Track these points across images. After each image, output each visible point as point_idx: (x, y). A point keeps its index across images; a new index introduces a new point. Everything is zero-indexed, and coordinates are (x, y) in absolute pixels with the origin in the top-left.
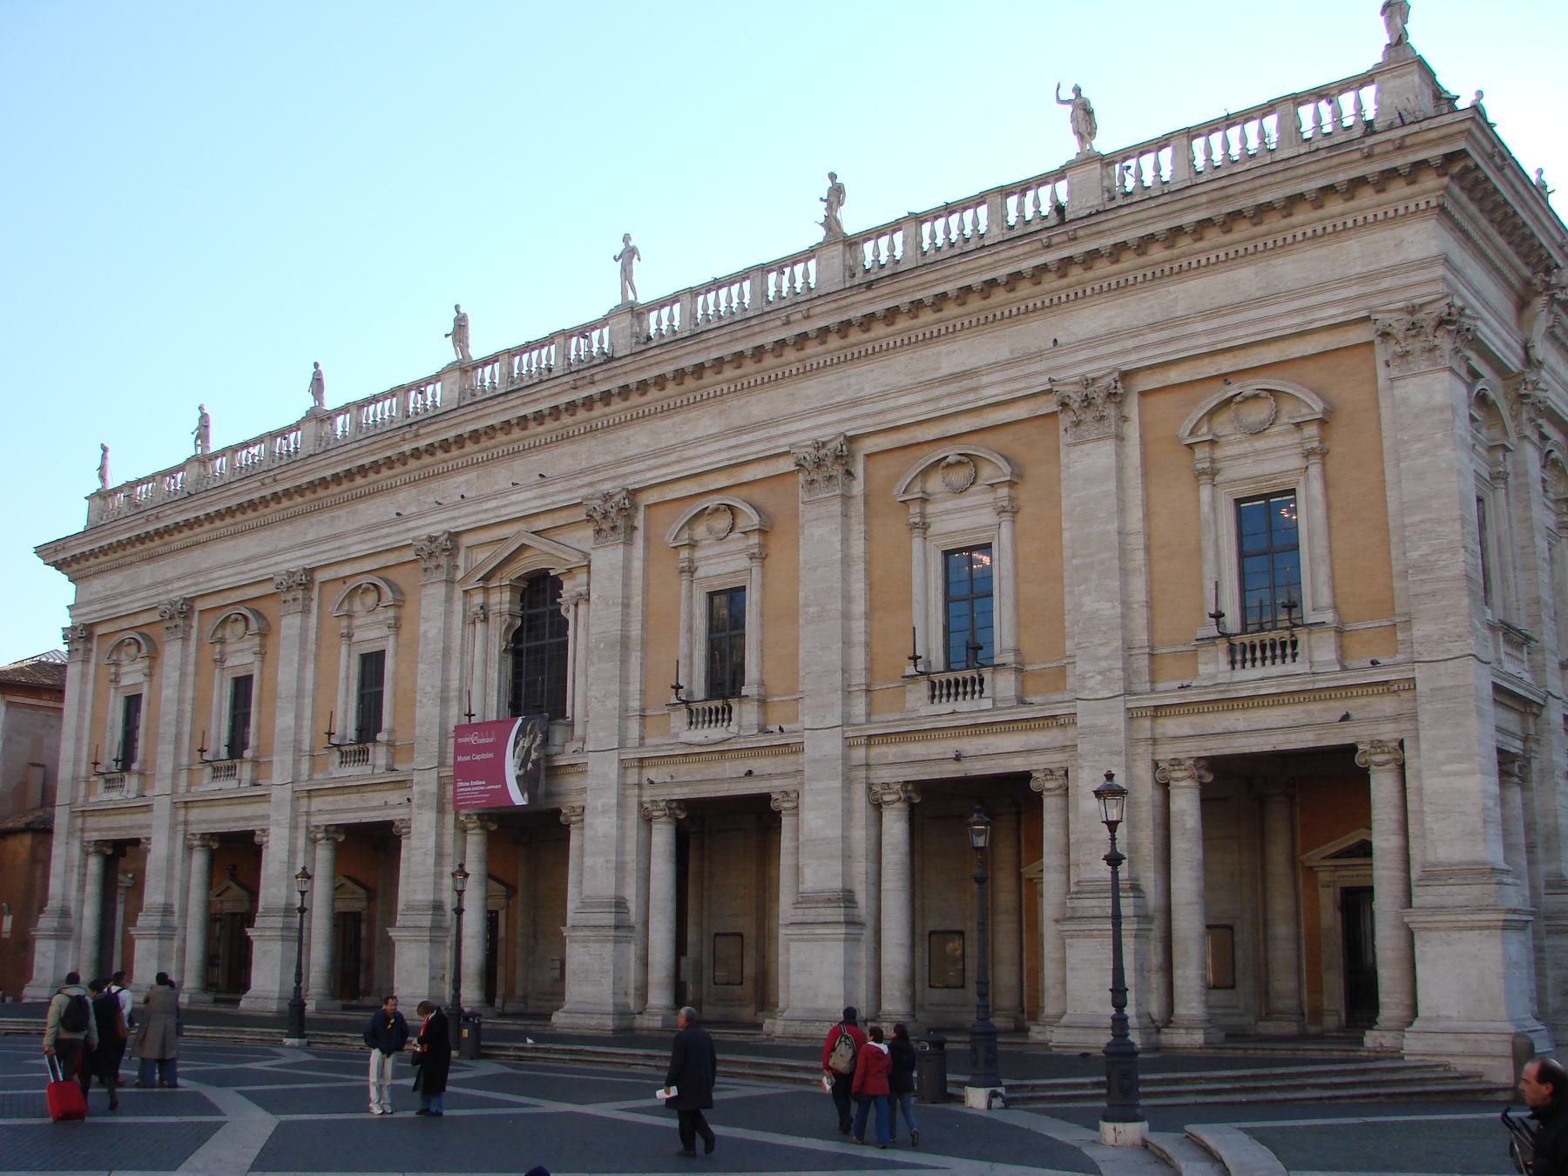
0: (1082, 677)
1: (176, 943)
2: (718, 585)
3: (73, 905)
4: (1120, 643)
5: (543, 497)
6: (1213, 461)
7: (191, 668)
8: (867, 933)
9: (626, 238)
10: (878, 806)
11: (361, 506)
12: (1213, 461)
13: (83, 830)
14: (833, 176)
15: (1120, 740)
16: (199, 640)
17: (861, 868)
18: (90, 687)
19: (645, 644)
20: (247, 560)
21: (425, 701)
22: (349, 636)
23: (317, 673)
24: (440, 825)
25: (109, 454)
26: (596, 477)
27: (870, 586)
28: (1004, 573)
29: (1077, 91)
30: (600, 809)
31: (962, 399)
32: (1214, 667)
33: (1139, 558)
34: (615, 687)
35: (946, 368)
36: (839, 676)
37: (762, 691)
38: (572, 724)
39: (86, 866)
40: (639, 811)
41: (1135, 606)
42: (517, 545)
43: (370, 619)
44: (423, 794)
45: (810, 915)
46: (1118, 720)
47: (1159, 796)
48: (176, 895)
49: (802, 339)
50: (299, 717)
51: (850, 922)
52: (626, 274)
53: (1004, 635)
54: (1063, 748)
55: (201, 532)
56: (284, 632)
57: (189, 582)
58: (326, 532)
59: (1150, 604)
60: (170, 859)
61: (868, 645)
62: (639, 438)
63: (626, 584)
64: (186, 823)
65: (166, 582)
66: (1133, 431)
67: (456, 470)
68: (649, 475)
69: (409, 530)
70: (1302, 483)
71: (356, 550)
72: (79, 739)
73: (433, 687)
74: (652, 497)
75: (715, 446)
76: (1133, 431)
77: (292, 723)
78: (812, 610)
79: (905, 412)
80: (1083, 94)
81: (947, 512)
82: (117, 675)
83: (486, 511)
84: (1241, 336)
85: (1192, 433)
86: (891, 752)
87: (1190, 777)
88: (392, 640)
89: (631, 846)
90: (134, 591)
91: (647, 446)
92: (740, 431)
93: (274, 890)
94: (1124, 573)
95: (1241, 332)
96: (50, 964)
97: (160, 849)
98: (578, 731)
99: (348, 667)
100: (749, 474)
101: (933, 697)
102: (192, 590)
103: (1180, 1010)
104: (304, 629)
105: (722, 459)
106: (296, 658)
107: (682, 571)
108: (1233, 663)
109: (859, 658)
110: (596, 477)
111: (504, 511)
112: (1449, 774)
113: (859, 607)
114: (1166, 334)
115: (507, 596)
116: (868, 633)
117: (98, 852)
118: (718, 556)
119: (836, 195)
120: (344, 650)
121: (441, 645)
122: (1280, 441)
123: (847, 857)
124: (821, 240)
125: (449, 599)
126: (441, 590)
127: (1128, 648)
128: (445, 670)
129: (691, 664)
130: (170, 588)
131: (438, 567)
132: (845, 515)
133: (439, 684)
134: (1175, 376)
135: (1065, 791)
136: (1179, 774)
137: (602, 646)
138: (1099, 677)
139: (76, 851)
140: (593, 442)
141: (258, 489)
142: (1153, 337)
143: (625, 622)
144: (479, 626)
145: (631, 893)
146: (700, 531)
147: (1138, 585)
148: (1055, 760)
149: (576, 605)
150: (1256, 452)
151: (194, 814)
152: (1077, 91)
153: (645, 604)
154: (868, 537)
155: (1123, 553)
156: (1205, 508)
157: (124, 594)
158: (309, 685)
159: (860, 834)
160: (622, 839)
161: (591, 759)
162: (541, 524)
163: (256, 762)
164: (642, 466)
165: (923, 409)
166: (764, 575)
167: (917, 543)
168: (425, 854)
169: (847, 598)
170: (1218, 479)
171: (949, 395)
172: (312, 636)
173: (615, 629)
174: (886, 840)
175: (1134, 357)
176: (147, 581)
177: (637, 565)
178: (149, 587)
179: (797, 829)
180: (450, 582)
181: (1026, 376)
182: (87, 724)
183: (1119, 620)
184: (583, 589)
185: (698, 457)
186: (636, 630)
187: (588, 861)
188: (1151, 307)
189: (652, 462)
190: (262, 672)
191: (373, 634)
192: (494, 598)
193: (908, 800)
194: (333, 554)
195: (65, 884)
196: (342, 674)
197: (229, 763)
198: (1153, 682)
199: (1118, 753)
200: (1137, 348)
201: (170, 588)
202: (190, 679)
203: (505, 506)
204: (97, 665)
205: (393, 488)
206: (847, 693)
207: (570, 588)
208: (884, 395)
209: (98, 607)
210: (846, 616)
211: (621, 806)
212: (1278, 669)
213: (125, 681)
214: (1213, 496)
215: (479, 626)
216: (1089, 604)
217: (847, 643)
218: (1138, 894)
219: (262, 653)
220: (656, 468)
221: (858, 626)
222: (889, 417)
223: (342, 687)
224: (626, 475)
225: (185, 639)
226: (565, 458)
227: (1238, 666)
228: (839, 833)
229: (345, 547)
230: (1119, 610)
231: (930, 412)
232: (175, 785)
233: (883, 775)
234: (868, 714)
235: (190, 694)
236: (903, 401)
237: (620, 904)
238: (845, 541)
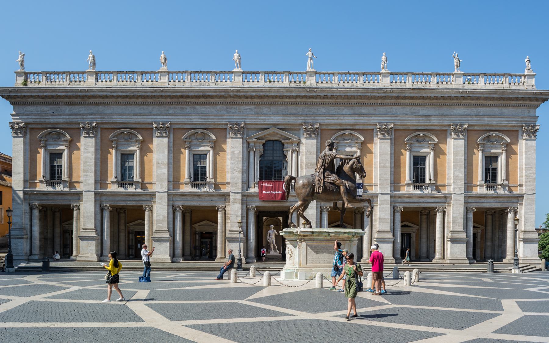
5: (284, 119)
26: (307, 118)
102: (100, 120)
110: (307, 118)
111: (267, 121)
112: (530, 214)
130: (85, 117)
162: (280, 127)
201: (85, 117)
220: (329, 119)
229: (191, 119)
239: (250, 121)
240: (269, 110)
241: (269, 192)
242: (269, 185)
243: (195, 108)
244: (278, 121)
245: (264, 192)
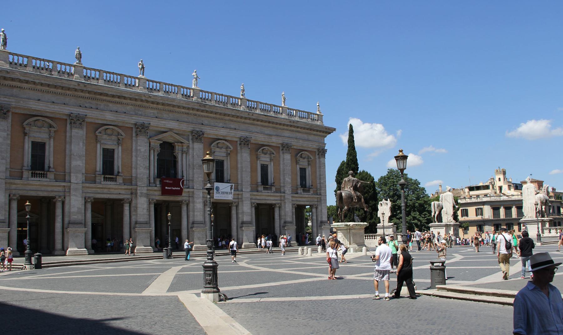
30: (198, 202)
35: (266, 132)
44: (141, 193)
73: (144, 165)
78: (244, 169)
137: (197, 166)
168: (143, 209)
207: (178, 147)
222: (257, 138)
239: (154, 123)
241: (170, 188)
242: (170, 182)
245: (166, 188)
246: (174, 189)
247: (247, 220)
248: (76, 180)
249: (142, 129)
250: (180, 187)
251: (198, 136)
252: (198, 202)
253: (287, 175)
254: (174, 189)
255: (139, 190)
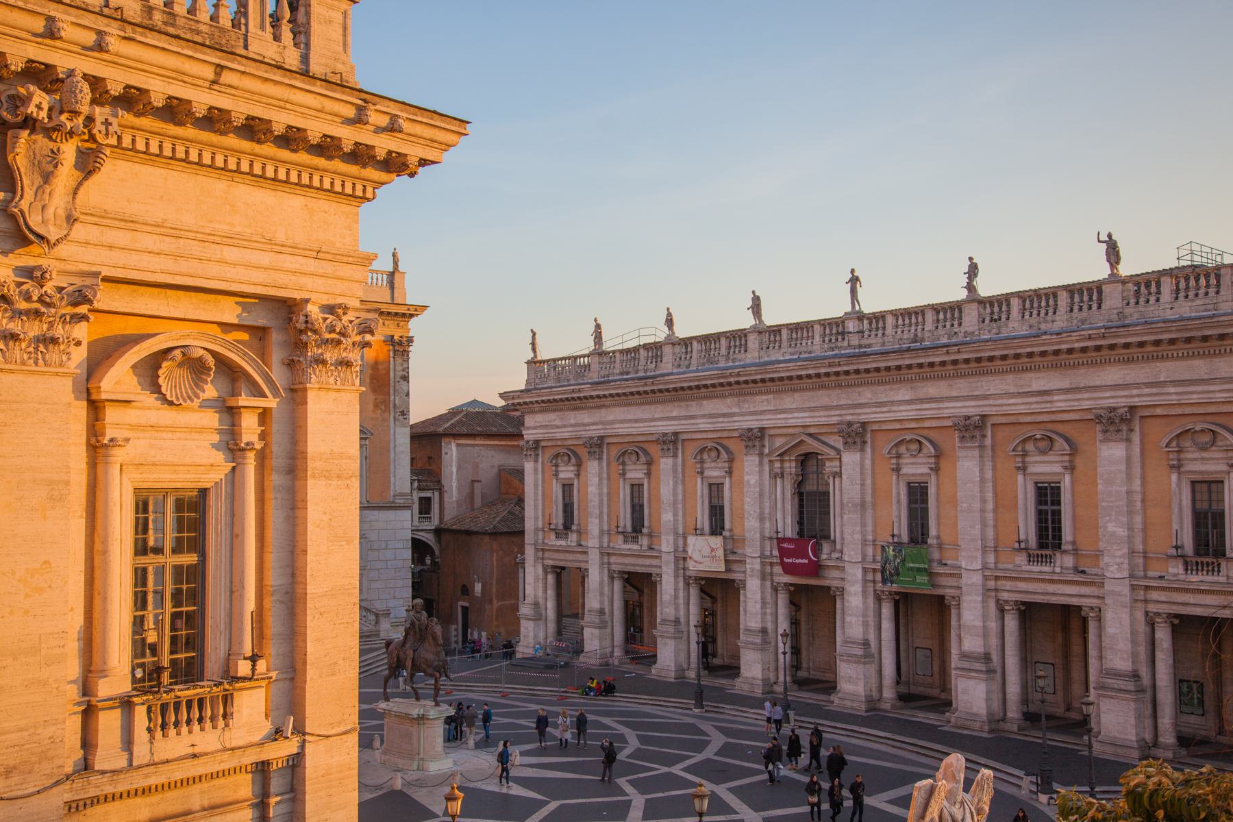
0: (1107, 564)
1: (608, 630)
2: (912, 479)
3: (541, 601)
4: (1127, 551)
6: (1179, 460)
7: (605, 475)
8: (998, 676)
9: (852, 271)
10: (1002, 611)
11: (705, 402)
12: (1179, 460)
13: (543, 559)
14: (971, 259)
15: (1127, 600)
16: (608, 459)
17: (994, 641)
18: (540, 476)
19: (874, 505)
20: (636, 421)
21: (751, 519)
22: (702, 473)
23: (684, 491)
24: (763, 586)
25: (536, 336)
27: (996, 494)
28: (1067, 502)
29: (1110, 236)
31: (1043, 406)
32: (1176, 569)
33: (1139, 504)
34: (858, 529)
35: (1035, 386)
36: (980, 542)
37: (939, 541)
38: (834, 542)
39: (546, 579)
40: (874, 595)
41: (1136, 530)
42: (798, 440)
43: (713, 465)
44: (752, 570)
45: (966, 665)
46: (1126, 590)
47: (1148, 629)
48: (606, 603)
49: (955, 362)
50: (675, 515)
51: (990, 671)
52: (854, 292)
53: (1067, 534)
54: (1099, 597)
55: (608, 402)
56: (662, 466)
57: (600, 427)
58: (683, 413)
59: (1144, 530)
60: (601, 583)
61: (995, 526)
62: (866, 395)
63: (862, 473)
64: (609, 564)
65: (584, 425)
66: (1136, 438)
67: (761, 393)
68: (872, 416)
69: (735, 421)
70: (1227, 479)
71: (703, 427)
72: (536, 507)
74: (875, 427)
75: (909, 407)
76: (1136, 438)
77: (672, 519)
78: (964, 505)
79: (1013, 408)
80: (1114, 238)
81: (1036, 462)
82: (557, 471)
83: (780, 419)
84: (1194, 398)
85: (1167, 446)
86: (1009, 585)
87: (1166, 622)
88: (727, 479)
89: (871, 613)
90: (565, 426)
91: (871, 399)
92: (922, 401)
93: (667, 610)
94: (1130, 513)
95: (1195, 396)
96: (531, 634)
97: (595, 577)
98: (838, 547)
99: (702, 490)
100: (927, 424)
101: (1030, 561)
103: (1161, 739)
104: (675, 465)
105: (913, 415)
106: (671, 482)
107: (893, 470)
108: (1186, 570)
109: (990, 533)
110: (843, 412)
113: (990, 506)
114: (1154, 390)
115: (793, 464)
116: (996, 520)
117: (552, 572)
118: (912, 464)
119: (973, 271)
120: (699, 480)
121: (758, 489)
122: (1216, 455)
123: (985, 635)
124: (964, 297)
125: (761, 464)
126: (757, 459)
127: (1132, 552)
128: (761, 503)
129: (900, 520)
130: (588, 428)
131: (754, 446)
132: (981, 456)
133: (758, 511)
134: (1159, 411)
135: (1099, 619)
136: (1159, 620)
138: (1116, 566)
139: (540, 571)
140: (840, 391)
141: (642, 386)
142: (1147, 391)
143: (863, 493)
144: (779, 481)
145: (872, 637)
146: (902, 449)
147: (1138, 519)
148: (1094, 602)
149: (834, 478)
150: (1203, 459)
151: (613, 559)
152: (1110, 236)
153: (874, 484)
154: (994, 469)
155: (1130, 504)
156: (1174, 485)
157: (558, 427)
158: (680, 497)
159: (993, 625)
160: (866, 609)
161: (847, 565)
162: (812, 430)
163: (650, 535)
164: (868, 410)
165: (1022, 407)
166: (938, 480)
167: (1020, 478)
169: (983, 501)
170: (1182, 469)
171: (1036, 403)
172: (680, 469)
173: (857, 498)
174: (1006, 629)
175: (1136, 399)
176: (573, 422)
177: (868, 462)
178: (573, 426)
179: (959, 616)
180: (761, 454)
181: (1079, 400)
182: (540, 498)
183: (1126, 539)
184: (837, 470)
185: (900, 411)
186: (869, 498)
187: (848, 619)
188: (1146, 373)
189: (874, 409)
190: (649, 483)
191: (715, 473)
192: (787, 465)
193: (1019, 609)
194: (688, 427)
195: (535, 589)
196: (699, 494)
197: (634, 535)
198: (1145, 570)
199: (1126, 607)
200: (1138, 396)
201: (588, 428)
202: (605, 482)
203: (791, 418)
204: (543, 463)
205: (724, 396)
206: (984, 549)
207: (830, 467)
208: (1000, 396)
209: (541, 431)
210: (983, 511)
211: (864, 592)
212: (1210, 578)
213: (561, 475)
214: (1179, 479)
215: (778, 480)
216: (1111, 527)
217: (984, 525)
218: (1136, 679)
219: (649, 474)
221: (990, 516)
223: (699, 501)
224: (860, 414)
225: (600, 459)
226: (823, 398)
227: (1189, 572)
228: (982, 625)
229: (697, 424)
230: (1126, 534)
231: (1024, 409)
232: (601, 542)
233: (1005, 596)
234: (996, 563)
235: (605, 490)
236: (1012, 401)
237: (866, 643)
238: (982, 471)
240: (792, 400)
243: (701, 405)
244: (804, 420)
246: (797, 561)
247: (973, 649)
248: (667, 546)
249: (755, 438)
250: (808, 557)
251: (856, 435)
252: (853, 592)
253: (1114, 513)
254: (797, 561)
255: (749, 563)
